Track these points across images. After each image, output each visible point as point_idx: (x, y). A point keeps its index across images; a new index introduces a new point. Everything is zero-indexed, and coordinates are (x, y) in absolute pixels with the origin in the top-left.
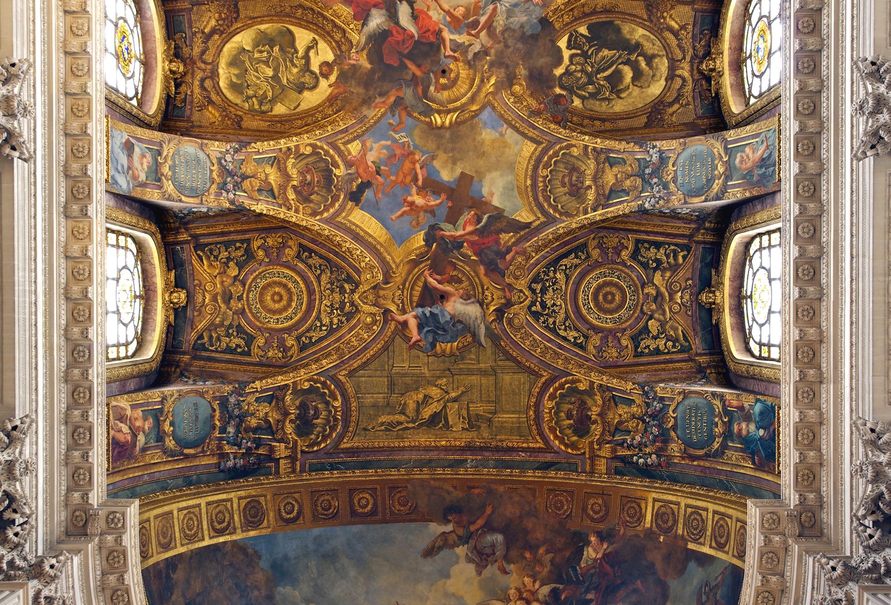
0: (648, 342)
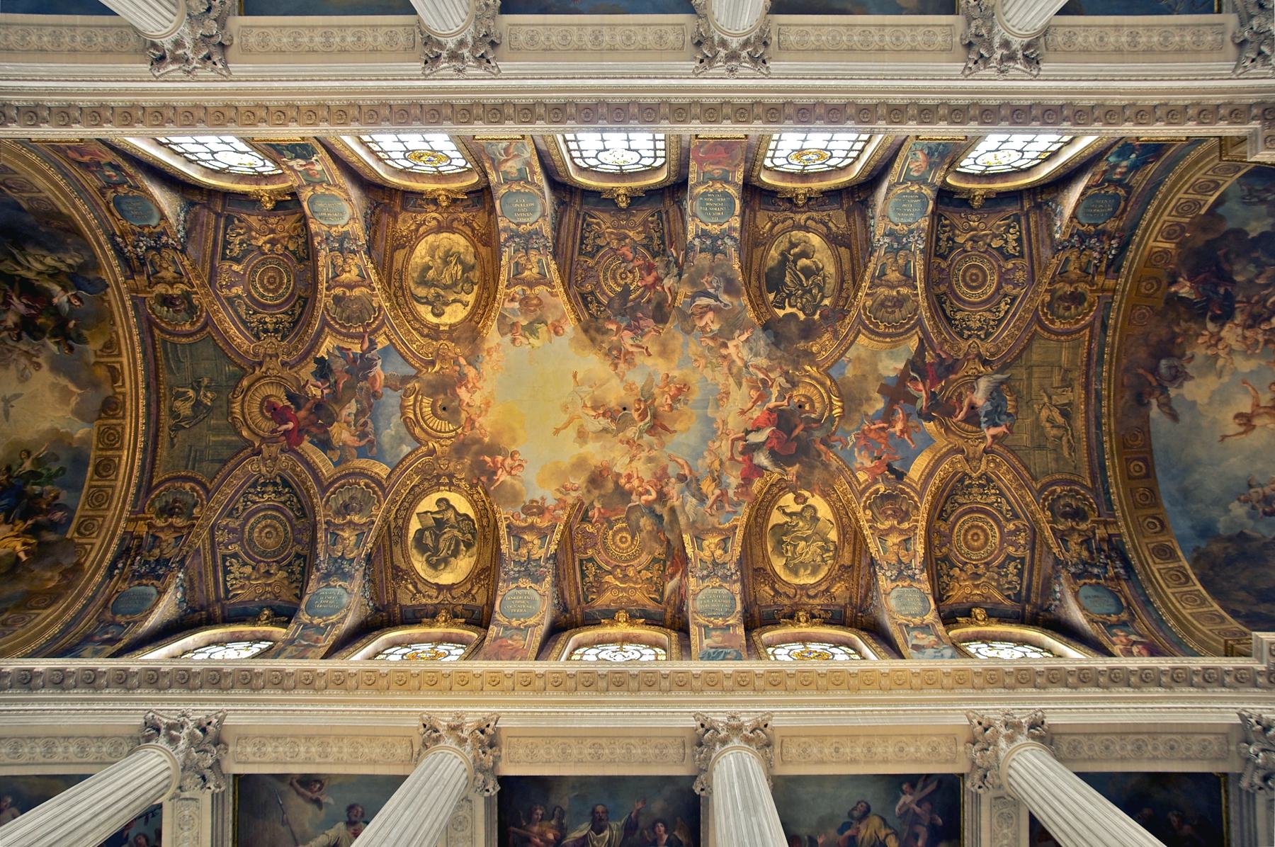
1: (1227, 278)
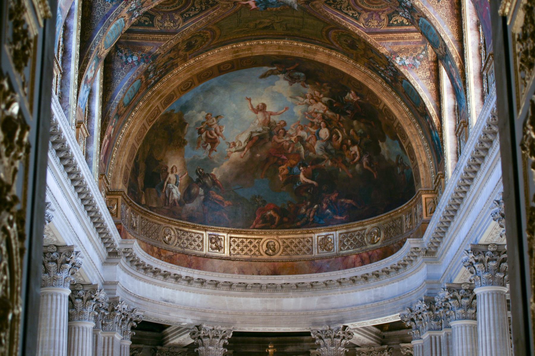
0: (397, 18)
1: (356, 116)
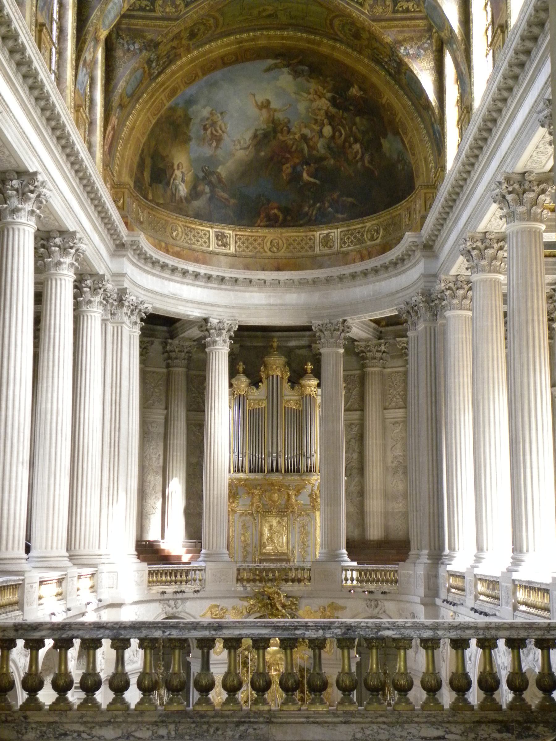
1: (360, 112)
